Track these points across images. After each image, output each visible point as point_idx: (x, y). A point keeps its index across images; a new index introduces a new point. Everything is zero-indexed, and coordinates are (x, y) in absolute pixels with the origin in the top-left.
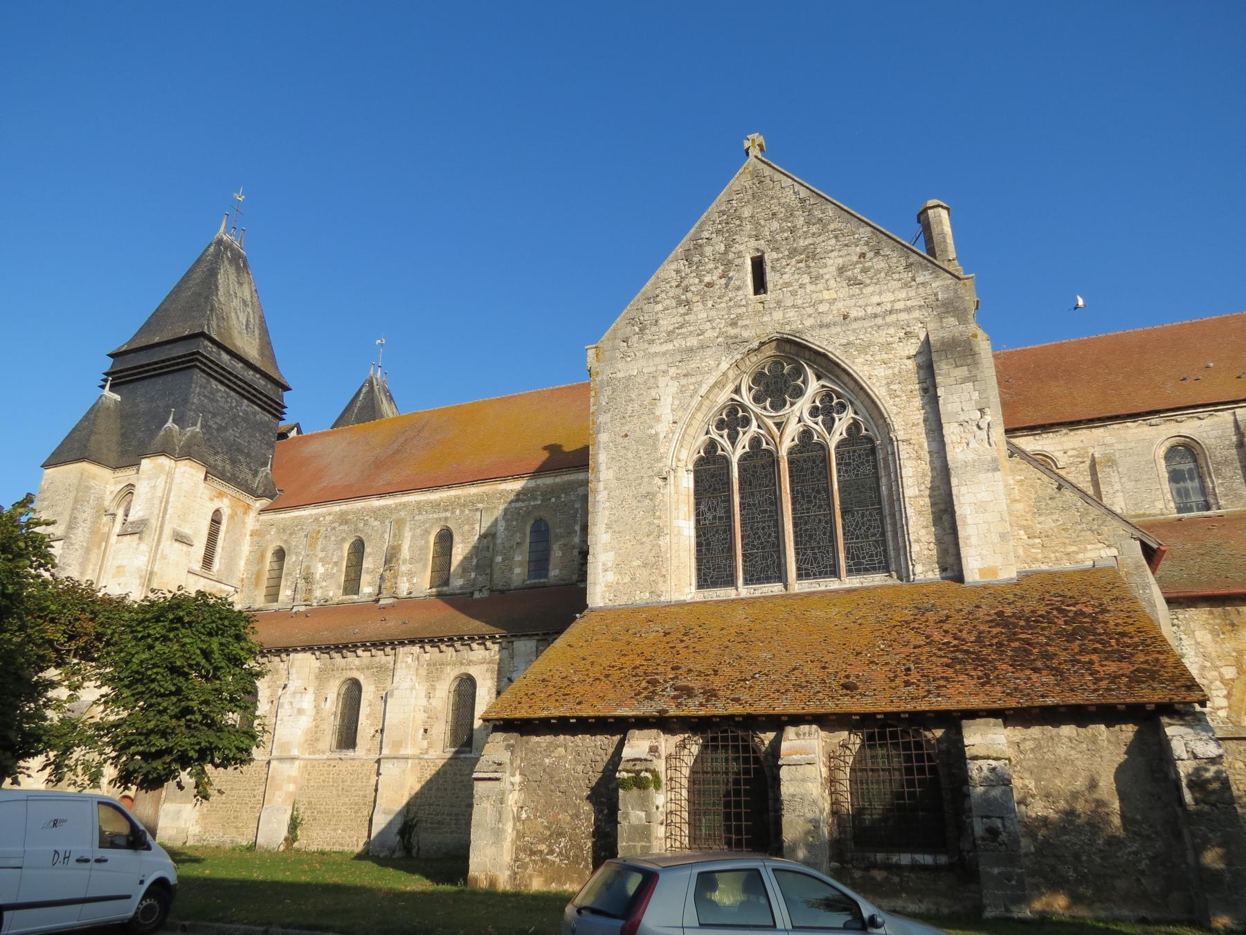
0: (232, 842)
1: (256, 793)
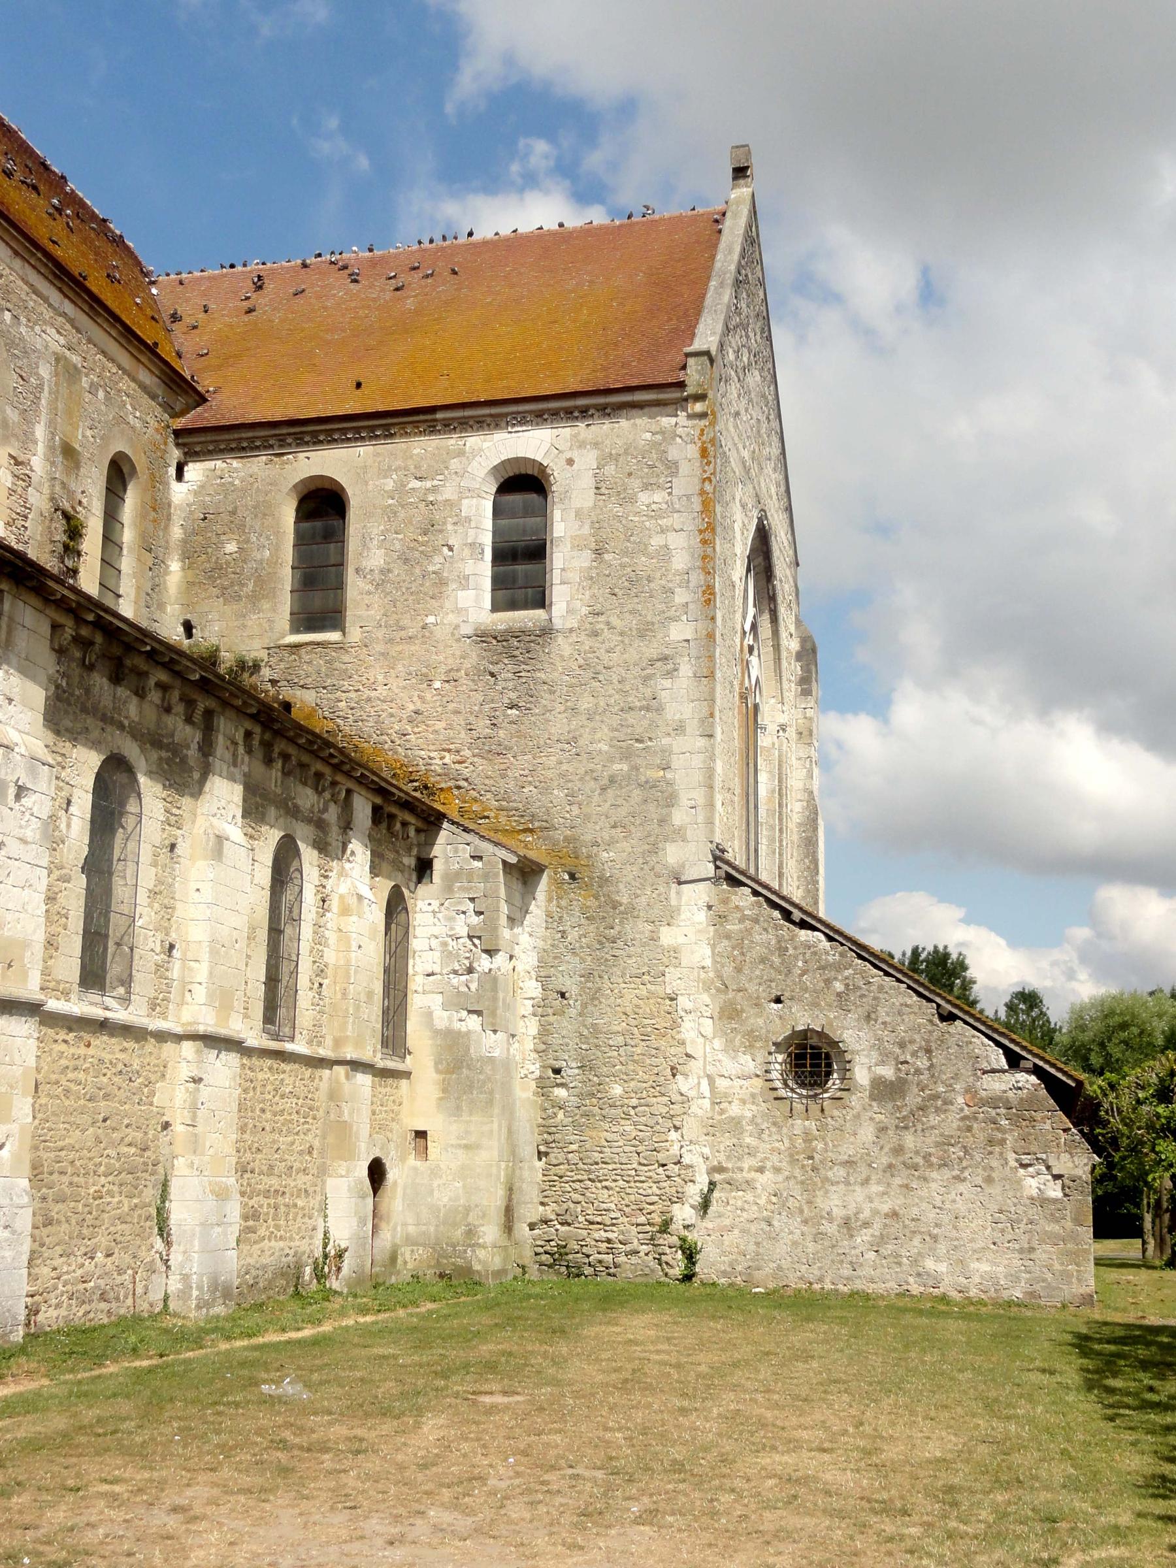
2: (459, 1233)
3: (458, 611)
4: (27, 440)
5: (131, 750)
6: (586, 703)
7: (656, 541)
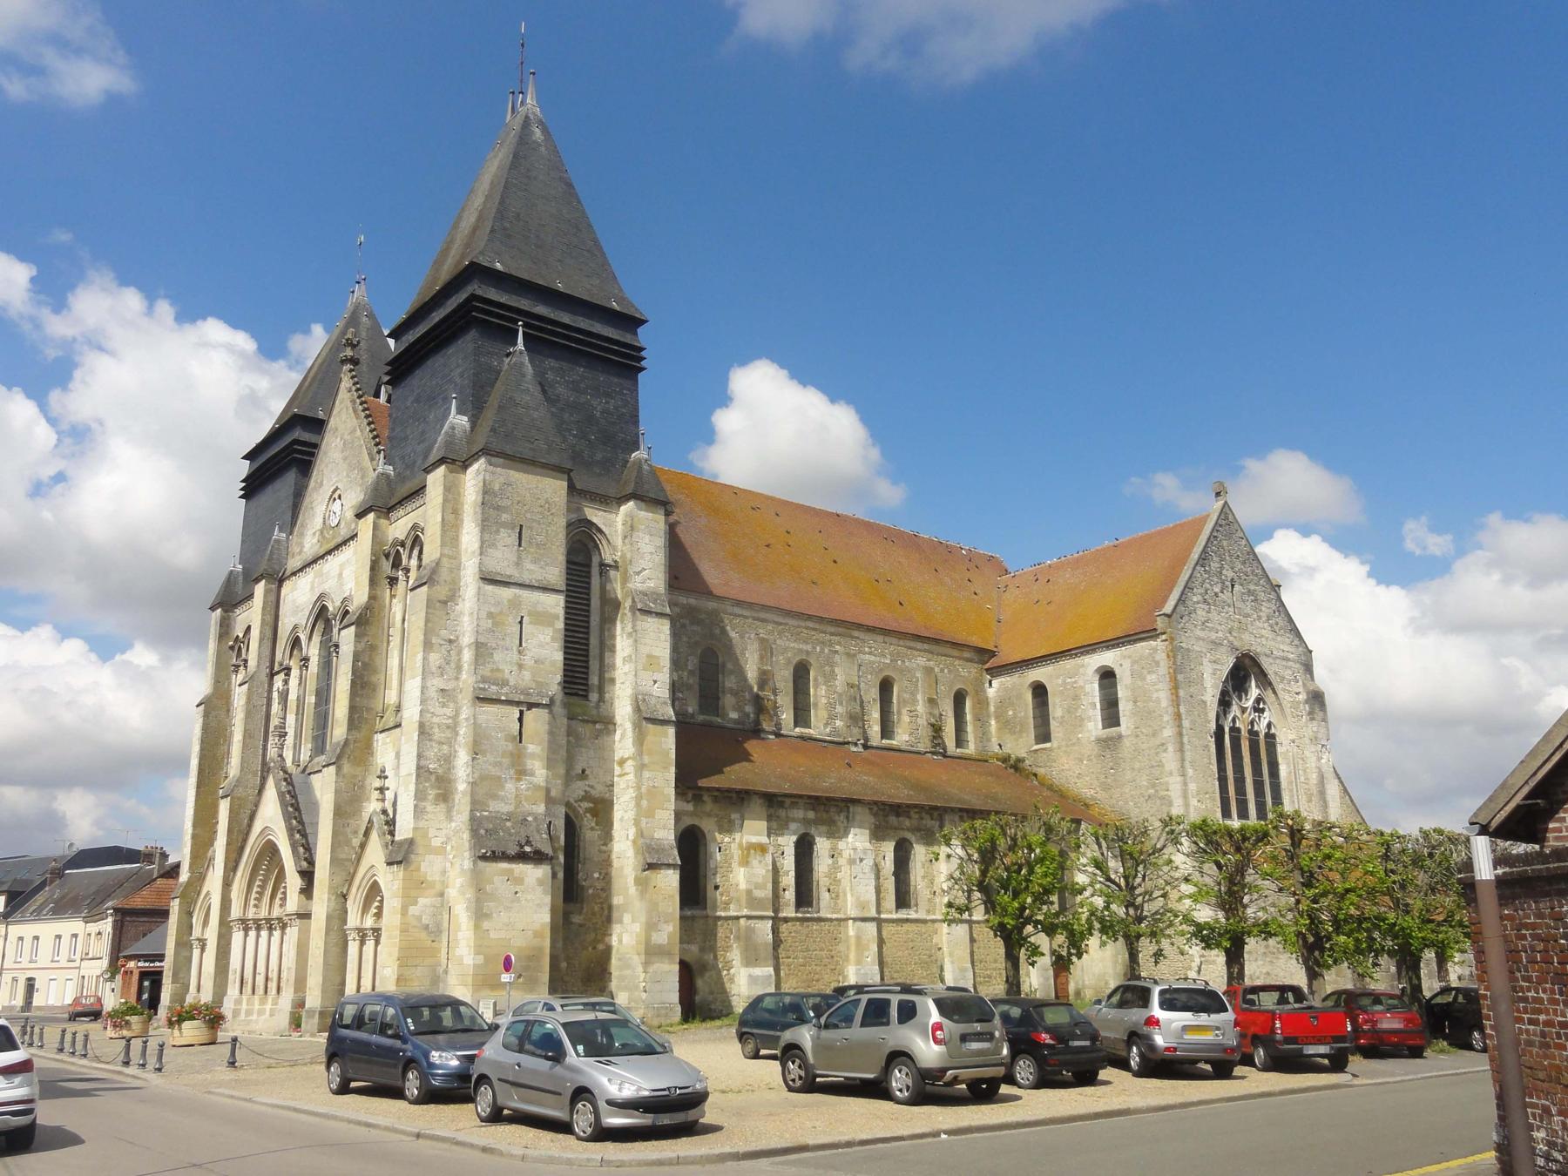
2: (1103, 983)
3: (1089, 731)
4: (915, 701)
5: (909, 835)
6: (1137, 765)
7: (1155, 695)
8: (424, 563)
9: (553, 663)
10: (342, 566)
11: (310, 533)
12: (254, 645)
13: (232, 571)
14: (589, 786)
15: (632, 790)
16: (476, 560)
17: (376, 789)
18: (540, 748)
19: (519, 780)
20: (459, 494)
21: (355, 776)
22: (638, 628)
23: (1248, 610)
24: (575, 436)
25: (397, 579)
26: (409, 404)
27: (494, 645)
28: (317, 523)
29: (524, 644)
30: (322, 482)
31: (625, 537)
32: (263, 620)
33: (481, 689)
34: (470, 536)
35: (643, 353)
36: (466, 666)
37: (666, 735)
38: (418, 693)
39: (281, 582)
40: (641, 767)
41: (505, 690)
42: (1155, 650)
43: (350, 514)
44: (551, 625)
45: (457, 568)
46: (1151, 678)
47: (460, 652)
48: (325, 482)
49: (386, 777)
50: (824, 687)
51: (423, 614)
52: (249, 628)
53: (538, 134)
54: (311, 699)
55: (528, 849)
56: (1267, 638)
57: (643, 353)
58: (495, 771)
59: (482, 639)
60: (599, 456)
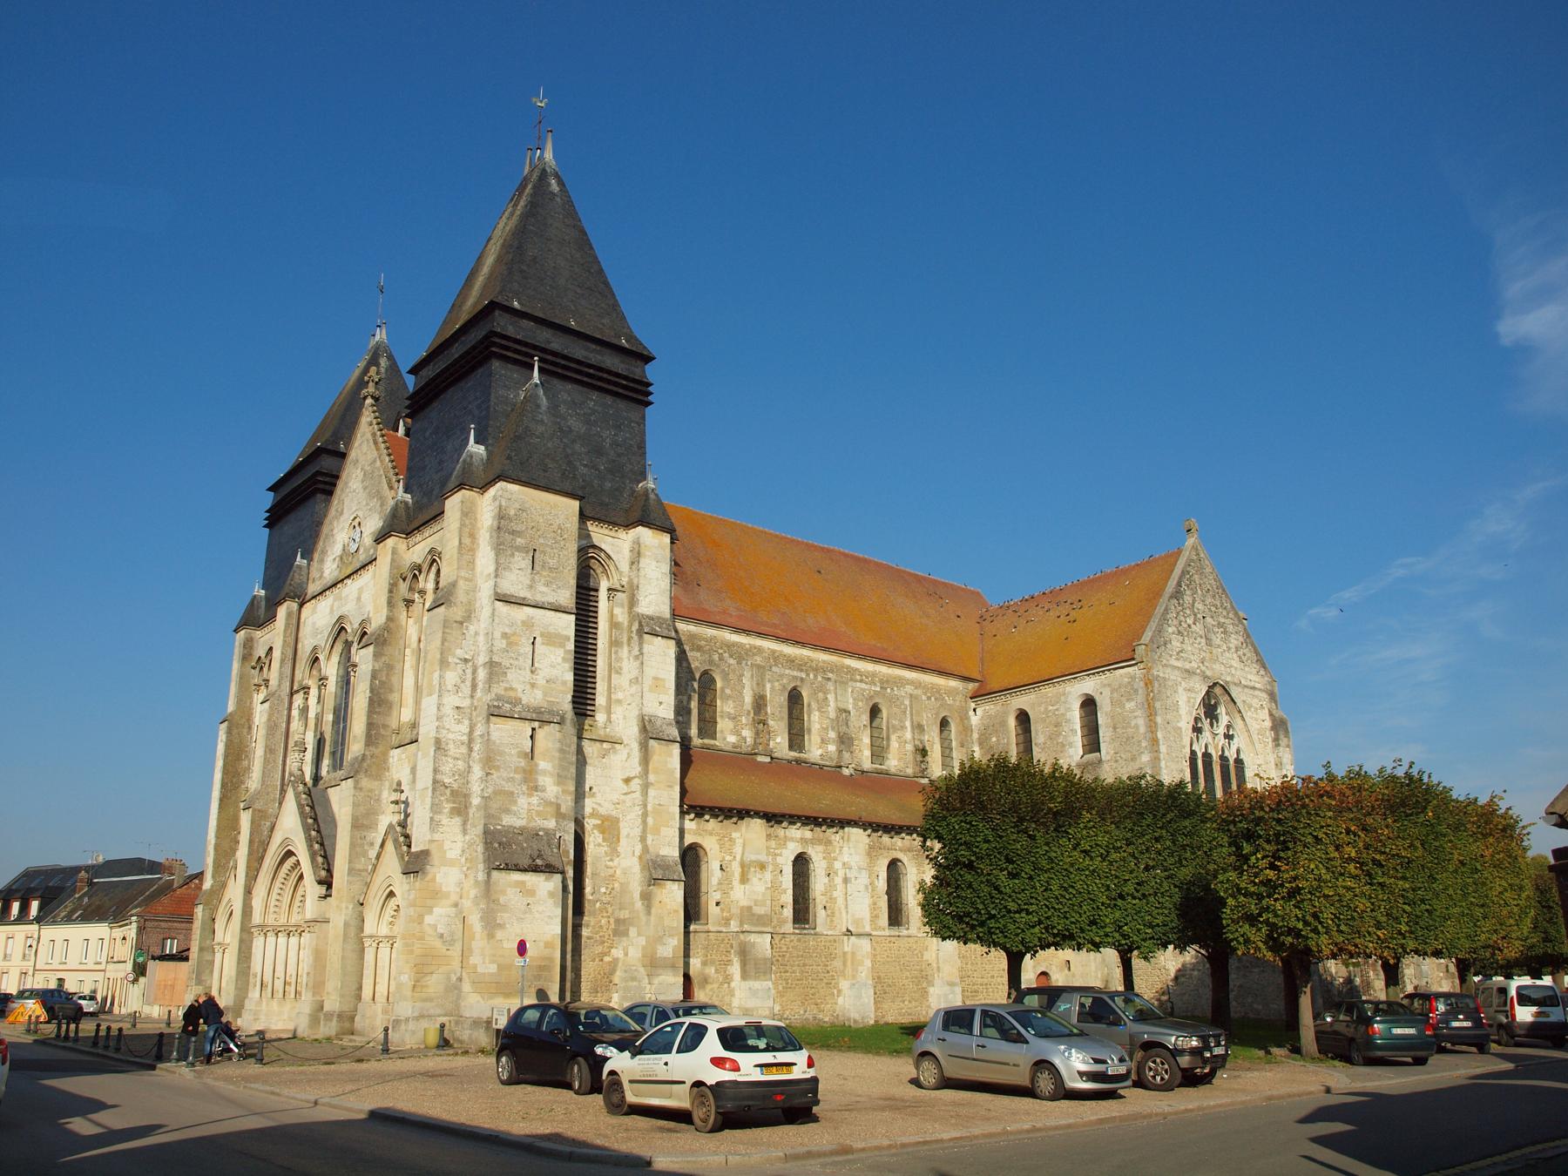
0: (815, 1018)
1: (829, 968)
3: (1070, 757)
4: (903, 728)
7: (1133, 724)
8: (441, 585)
9: (564, 683)
10: (361, 590)
11: (331, 558)
12: (276, 665)
13: (255, 596)
14: (596, 803)
15: (637, 808)
16: (492, 583)
17: (392, 802)
18: (550, 765)
19: (530, 795)
20: (476, 519)
21: (371, 791)
22: (645, 651)
23: (1218, 641)
24: (585, 466)
25: (413, 601)
26: (428, 434)
27: (508, 665)
28: (336, 550)
29: (536, 665)
30: (342, 510)
31: (633, 563)
32: (285, 641)
33: (494, 706)
34: (485, 558)
35: (650, 389)
36: (480, 685)
37: (671, 755)
38: (436, 709)
39: (301, 605)
40: (646, 787)
41: (518, 709)
42: (1133, 678)
43: (368, 540)
44: (562, 645)
45: (475, 589)
46: (1130, 705)
47: (474, 672)
48: (345, 511)
49: (402, 792)
50: (817, 713)
51: (440, 635)
52: (271, 649)
53: (554, 186)
54: (329, 717)
55: (539, 862)
56: (1236, 669)
57: (650, 389)
58: (508, 787)
59: (496, 659)
60: (608, 485)
